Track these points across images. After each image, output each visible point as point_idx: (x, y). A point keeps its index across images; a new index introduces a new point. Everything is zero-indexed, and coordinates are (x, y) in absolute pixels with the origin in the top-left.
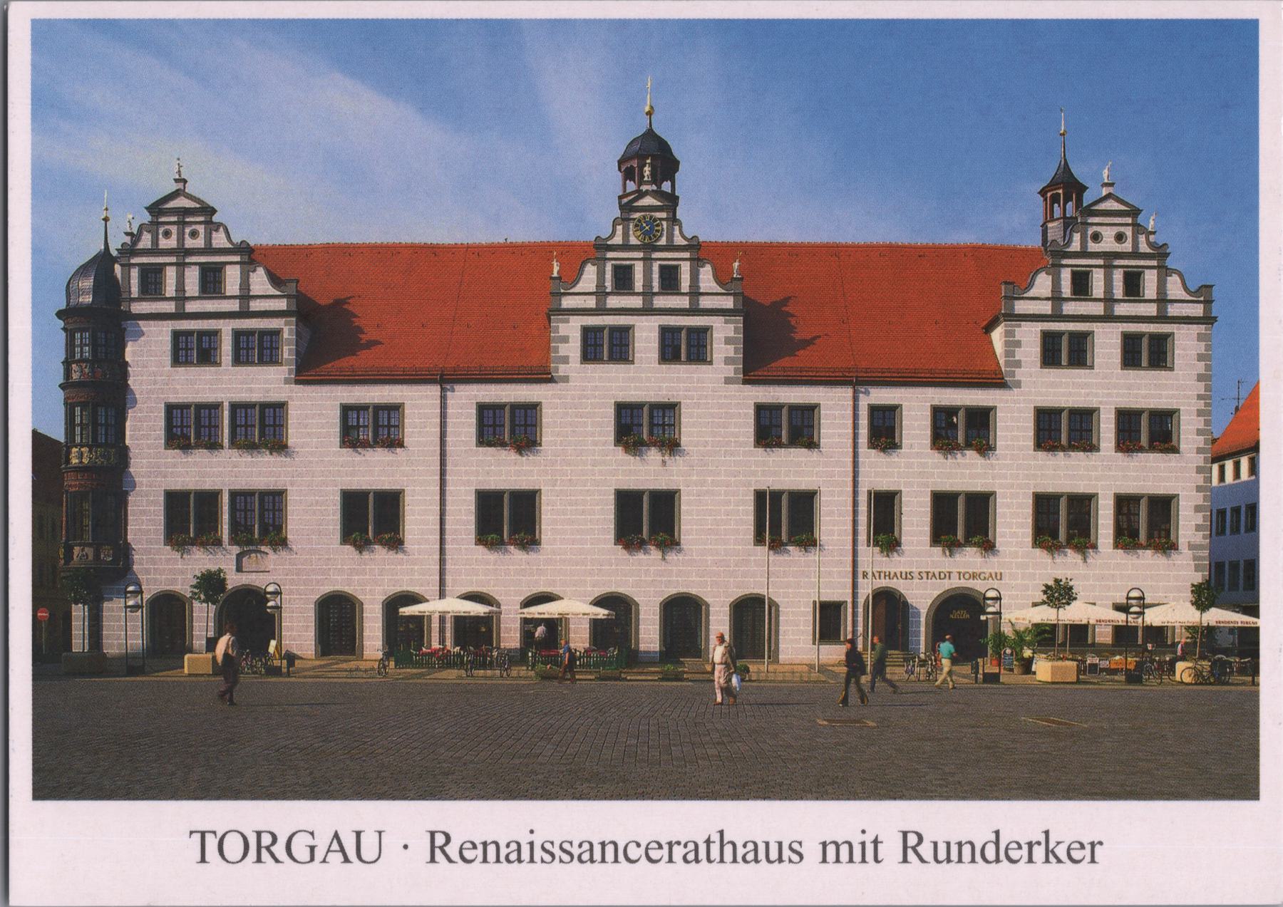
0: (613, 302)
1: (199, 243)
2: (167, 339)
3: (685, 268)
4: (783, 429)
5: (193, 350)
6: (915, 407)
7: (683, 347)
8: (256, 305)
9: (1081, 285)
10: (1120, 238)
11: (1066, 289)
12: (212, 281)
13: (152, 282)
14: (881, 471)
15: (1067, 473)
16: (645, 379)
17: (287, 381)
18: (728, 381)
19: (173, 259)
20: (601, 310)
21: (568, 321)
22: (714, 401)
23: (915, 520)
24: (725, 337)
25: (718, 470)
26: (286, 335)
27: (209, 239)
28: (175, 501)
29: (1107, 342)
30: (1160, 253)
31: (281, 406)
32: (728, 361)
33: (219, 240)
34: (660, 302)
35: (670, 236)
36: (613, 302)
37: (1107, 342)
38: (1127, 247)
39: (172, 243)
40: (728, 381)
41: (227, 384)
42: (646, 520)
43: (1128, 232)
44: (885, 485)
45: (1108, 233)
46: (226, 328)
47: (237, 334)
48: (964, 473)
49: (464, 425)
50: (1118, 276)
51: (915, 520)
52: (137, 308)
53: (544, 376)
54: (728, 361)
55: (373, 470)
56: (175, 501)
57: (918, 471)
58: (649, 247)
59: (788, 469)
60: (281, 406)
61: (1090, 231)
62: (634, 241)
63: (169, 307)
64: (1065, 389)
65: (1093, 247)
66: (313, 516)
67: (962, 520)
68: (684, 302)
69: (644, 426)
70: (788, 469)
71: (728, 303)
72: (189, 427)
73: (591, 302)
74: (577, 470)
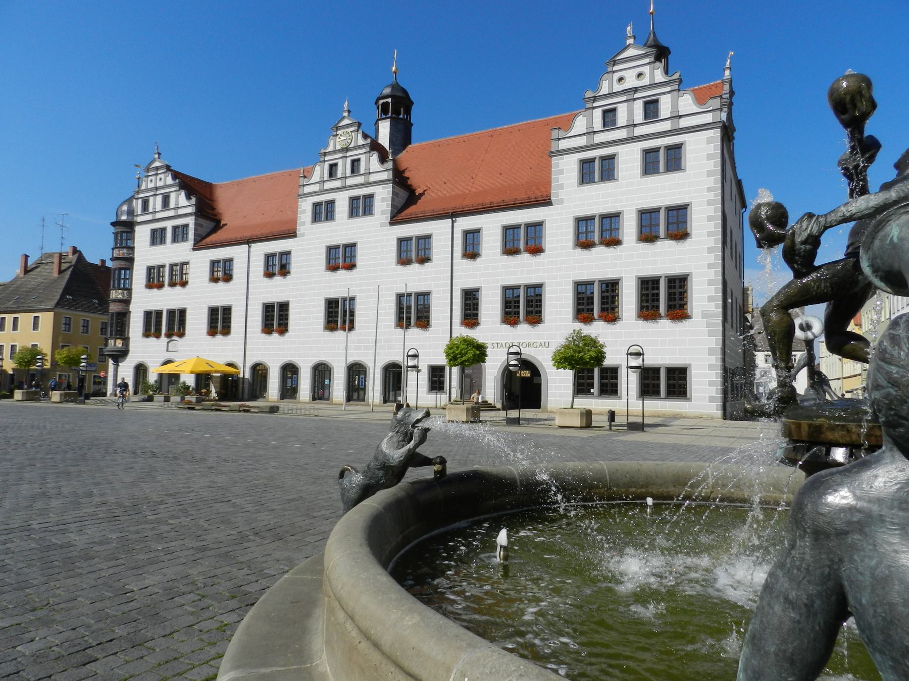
0: (328, 185)
3: (363, 158)
4: (414, 252)
5: (157, 237)
6: (491, 226)
7: (361, 206)
9: (609, 116)
11: (598, 124)
14: (469, 274)
15: (599, 264)
16: (343, 228)
18: (382, 225)
21: (305, 201)
22: (376, 236)
23: (491, 307)
24: (383, 197)
25: (377, 282)
29: (629, 159)
32: (383, 213)
34: (350, 182)
36: (328, 185)
37: (629, 159)
38: (645, 81)
40: (382, 225)
42: (338, 314)
44: (470, 285)
46: (169, 225)
47: (175, 228)
48: (522, 270)
49: (258, 266)
50: (639, 106)
51: (491, 307)
52: (139, 219)
53: (291, 234)
54: (383, 213)
57: (495, 272)
59: (414, 279)
61: (616, 76)
64: (597, 199)
65: (617, 88)
67: (523, 305)
70: (414, 279)
72: (154, 280)
74: (307, 288)
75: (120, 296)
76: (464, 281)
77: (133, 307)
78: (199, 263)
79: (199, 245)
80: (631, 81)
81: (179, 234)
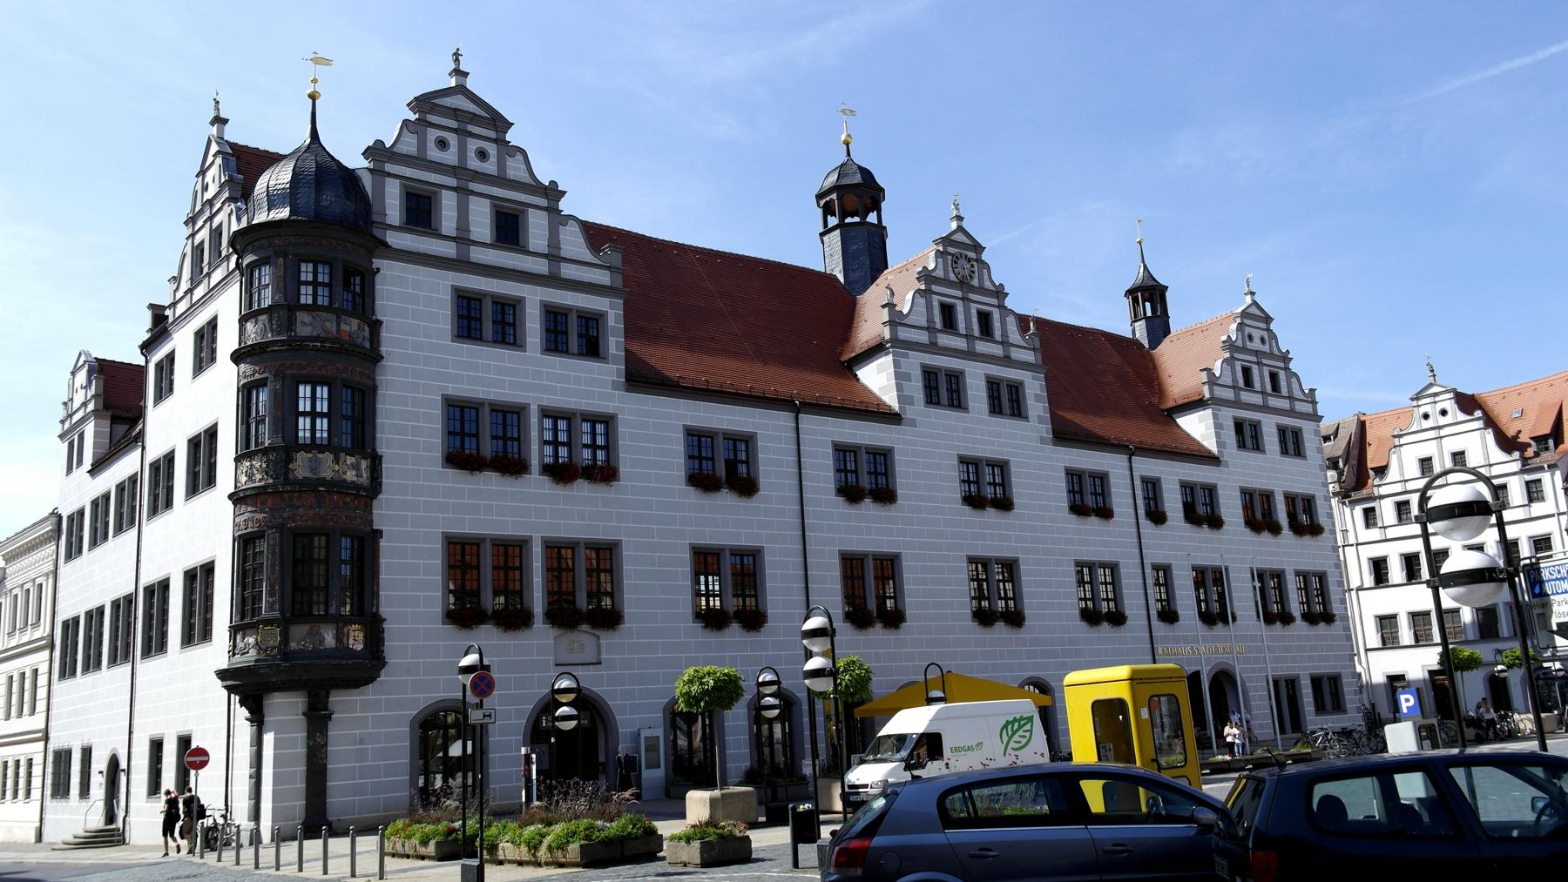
0: (945, 340)
1: (490, 167)
2: (446, 297)
5: (484, 320)
8: (568, 271)
10: (1263, 340)
12: (509, 229)
13: (420, 211)
17: (615, 385)
19: (453, 182)
20: (932, 348)
26: (611, 322)
27: (501, 164)
28: (461, 554)
30: (1285, 358)
31: (608, 421)
33: (515, 170)
35: (981, 279)
39: (450, 157)
41: (529, 377)
43: (1265, 334)
45: (1257, 334)
52: (395, 239)
55: (725, 521)
56: (461, 554)
58: (963, 284)
60: (608, 421)
62: (952, 277)
63: (448, 250)
65: (1249, 345)
66: (656, 588)
68: (997, 350)
69: (986, 487)
71: (1029, 357)
72: (480, 439)
73: (923, 337)
75: (350, 476)
76: (1154, 555)
77: (384, 513)
78: (654, 431)
79: (640, 378)
80: (1256, 345)
81: (572, 335)
